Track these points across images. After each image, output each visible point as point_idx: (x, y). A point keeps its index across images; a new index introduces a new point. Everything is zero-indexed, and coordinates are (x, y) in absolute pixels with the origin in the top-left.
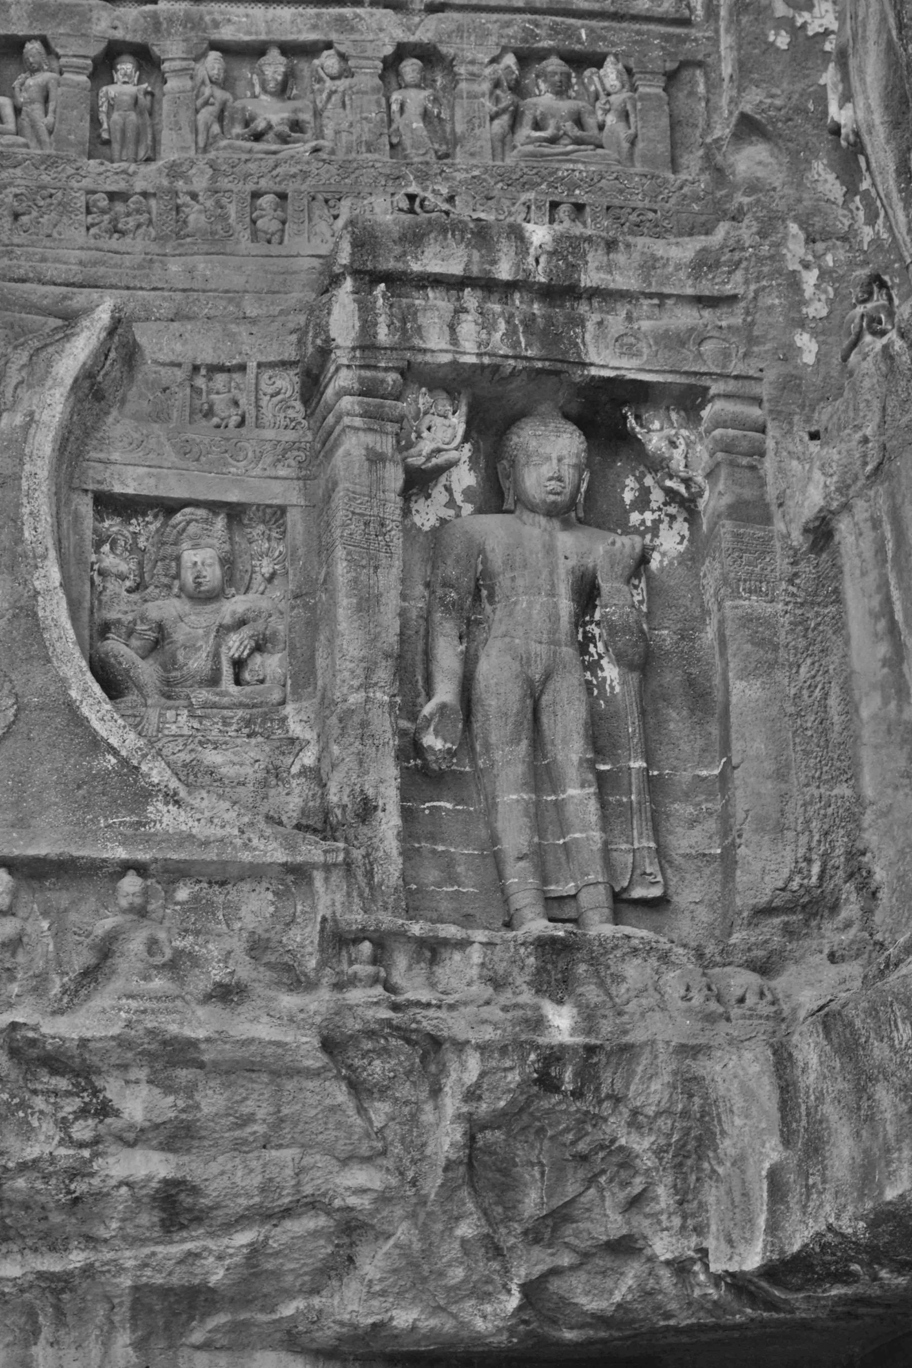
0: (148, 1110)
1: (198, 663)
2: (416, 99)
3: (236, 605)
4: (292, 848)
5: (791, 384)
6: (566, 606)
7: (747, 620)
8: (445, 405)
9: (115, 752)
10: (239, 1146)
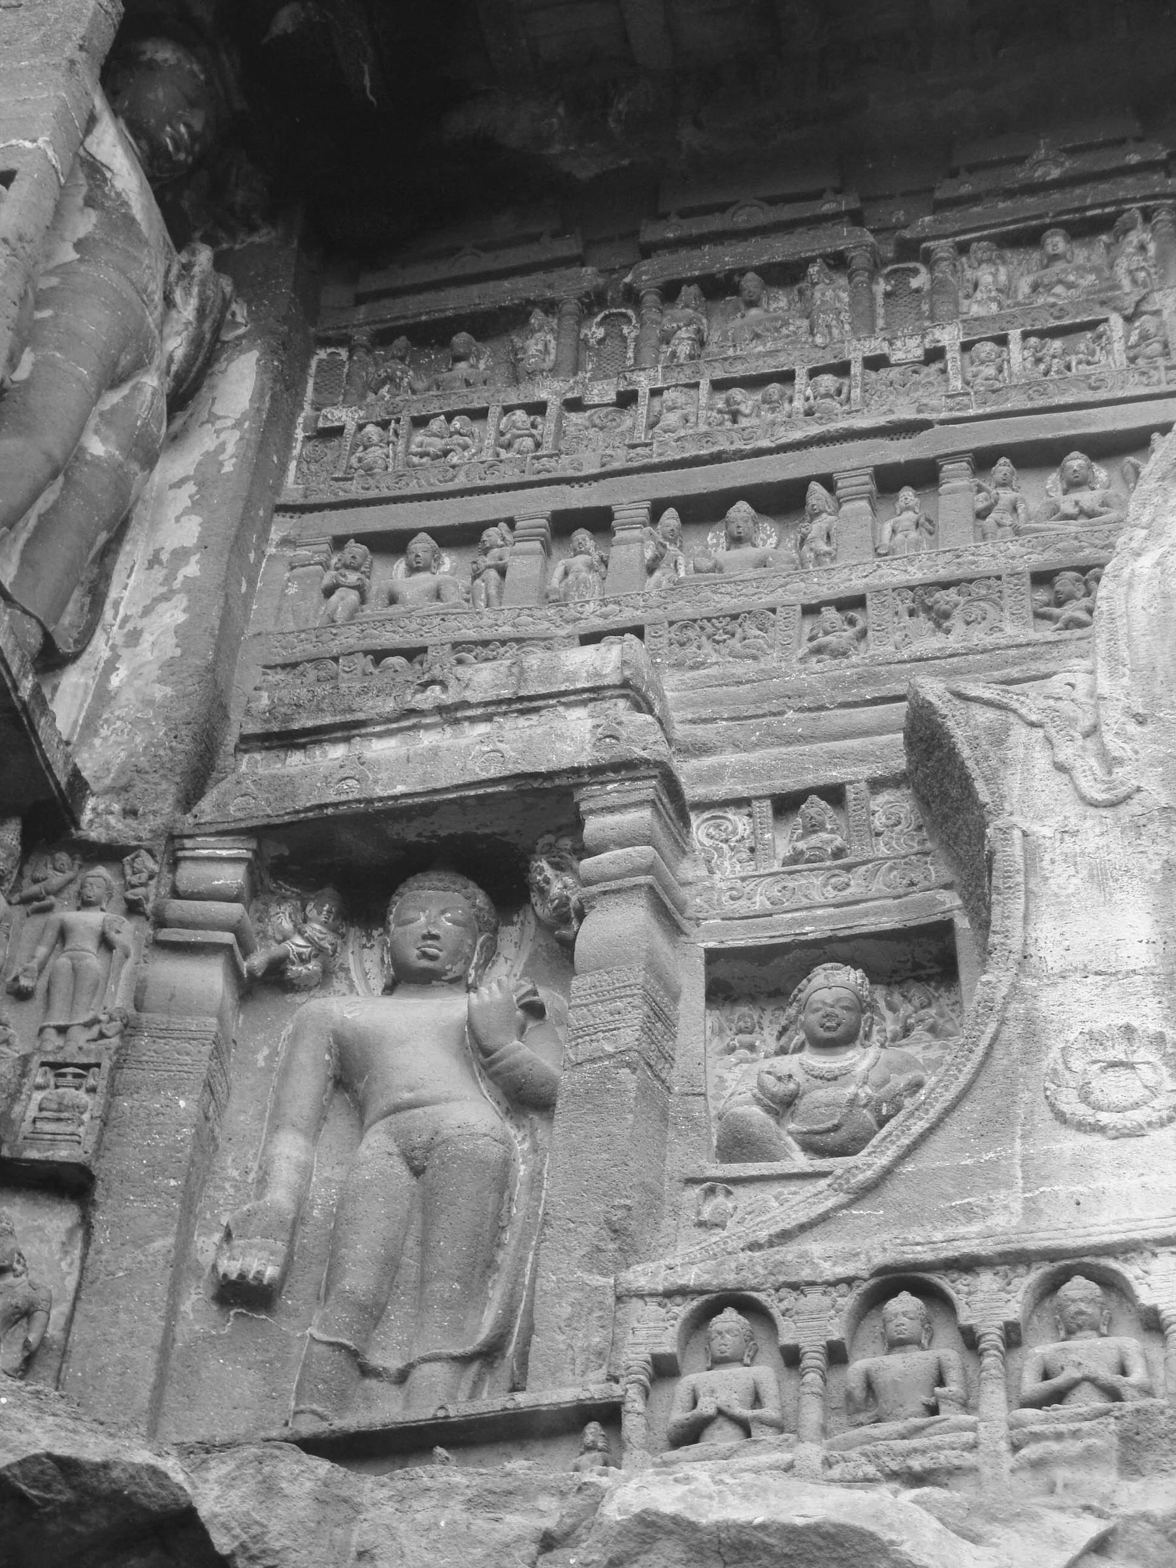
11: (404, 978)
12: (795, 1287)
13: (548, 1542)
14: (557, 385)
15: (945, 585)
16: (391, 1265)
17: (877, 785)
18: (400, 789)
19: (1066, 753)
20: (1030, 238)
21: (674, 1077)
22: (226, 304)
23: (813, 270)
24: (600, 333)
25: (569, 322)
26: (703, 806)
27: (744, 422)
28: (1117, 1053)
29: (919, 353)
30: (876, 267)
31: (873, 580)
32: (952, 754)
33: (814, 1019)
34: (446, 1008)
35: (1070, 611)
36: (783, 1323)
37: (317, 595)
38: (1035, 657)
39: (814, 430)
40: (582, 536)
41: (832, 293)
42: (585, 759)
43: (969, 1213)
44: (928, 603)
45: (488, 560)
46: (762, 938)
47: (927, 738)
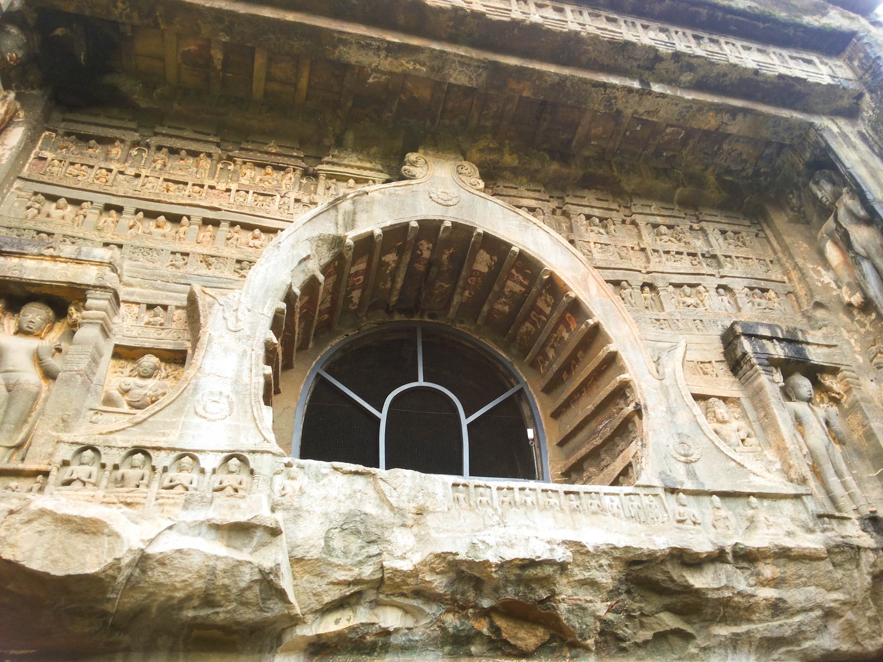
0: (773, 573)
2: (725, 298)
4: (797, 489)
5: (859, 367)
8: (775, 371)
9: (734, 461)
10: (797, 586)
11: (20, 331)
12: (110, 447)
13: (11, 512)
14: (118, 165)
15: (213, 257)
17: (177, 307)
18: (32, 277)
19: (227, 315)
20: (263, 166)
21: (95, 379)
22: (17, 111)
23: (202, 155)
24: (136, 153)
25: (127, 148)
26: (125, 302)
27: (170, 193)
28: (216, 399)
29: (224, 189)
30: (220, 160)
31: (193, 250)
32: (197, 307)
33: (141, 369)
34: (32, 343)
35: (243, 272)
36: (103, 456)
37: (24, 208)
38: (231, 283)
39: (189, 202)
40: (113, 212)
41: (206, 163)
42: (92, 283)
43: (164, 434)
44: (207, 260)
45: (81, 212)
46: (132, 344)
47: (192, 300)
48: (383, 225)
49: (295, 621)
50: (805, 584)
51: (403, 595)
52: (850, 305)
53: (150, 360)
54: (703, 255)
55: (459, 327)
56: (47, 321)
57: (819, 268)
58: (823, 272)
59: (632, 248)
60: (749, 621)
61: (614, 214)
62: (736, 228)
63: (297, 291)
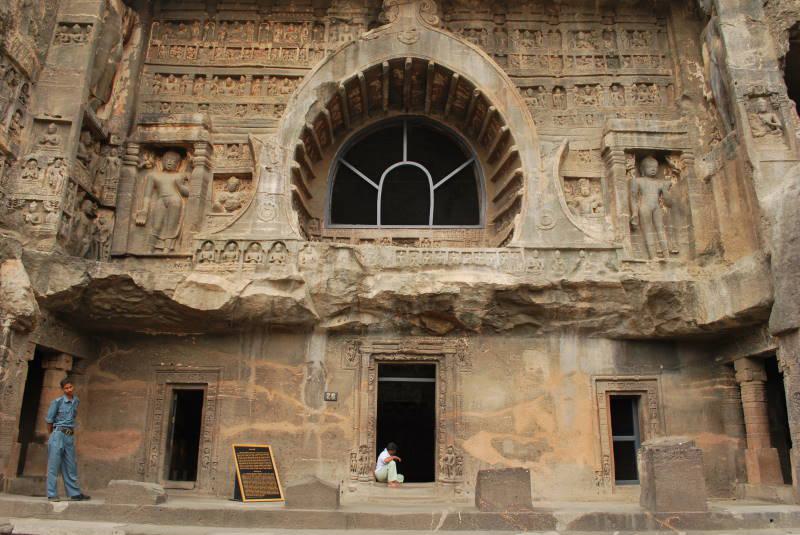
1: (587, 209)
2: (616, 94)
3: (592, 198)
6: (657, 195)
7: (694, 197)
10: (602, 301)
16: (162, 223)
17: (244, 144)
20: (287, 24)
26: (215, 144)
40: (201, 79)
41: (251, 29)
48: (364, 69)
49: (318, 322)
50: (608, 300)
51: (371, 308)
52: (706, 98)
53: (233, 181)
54: (608, 57)
55: (433, 117)
56: (176, 162)
57: (697, 64)
58: (698, 67)
59: (552, 56)
60: (573, 319)
61: (543, 25)
62: (641, 27)
63: (311, 126)
